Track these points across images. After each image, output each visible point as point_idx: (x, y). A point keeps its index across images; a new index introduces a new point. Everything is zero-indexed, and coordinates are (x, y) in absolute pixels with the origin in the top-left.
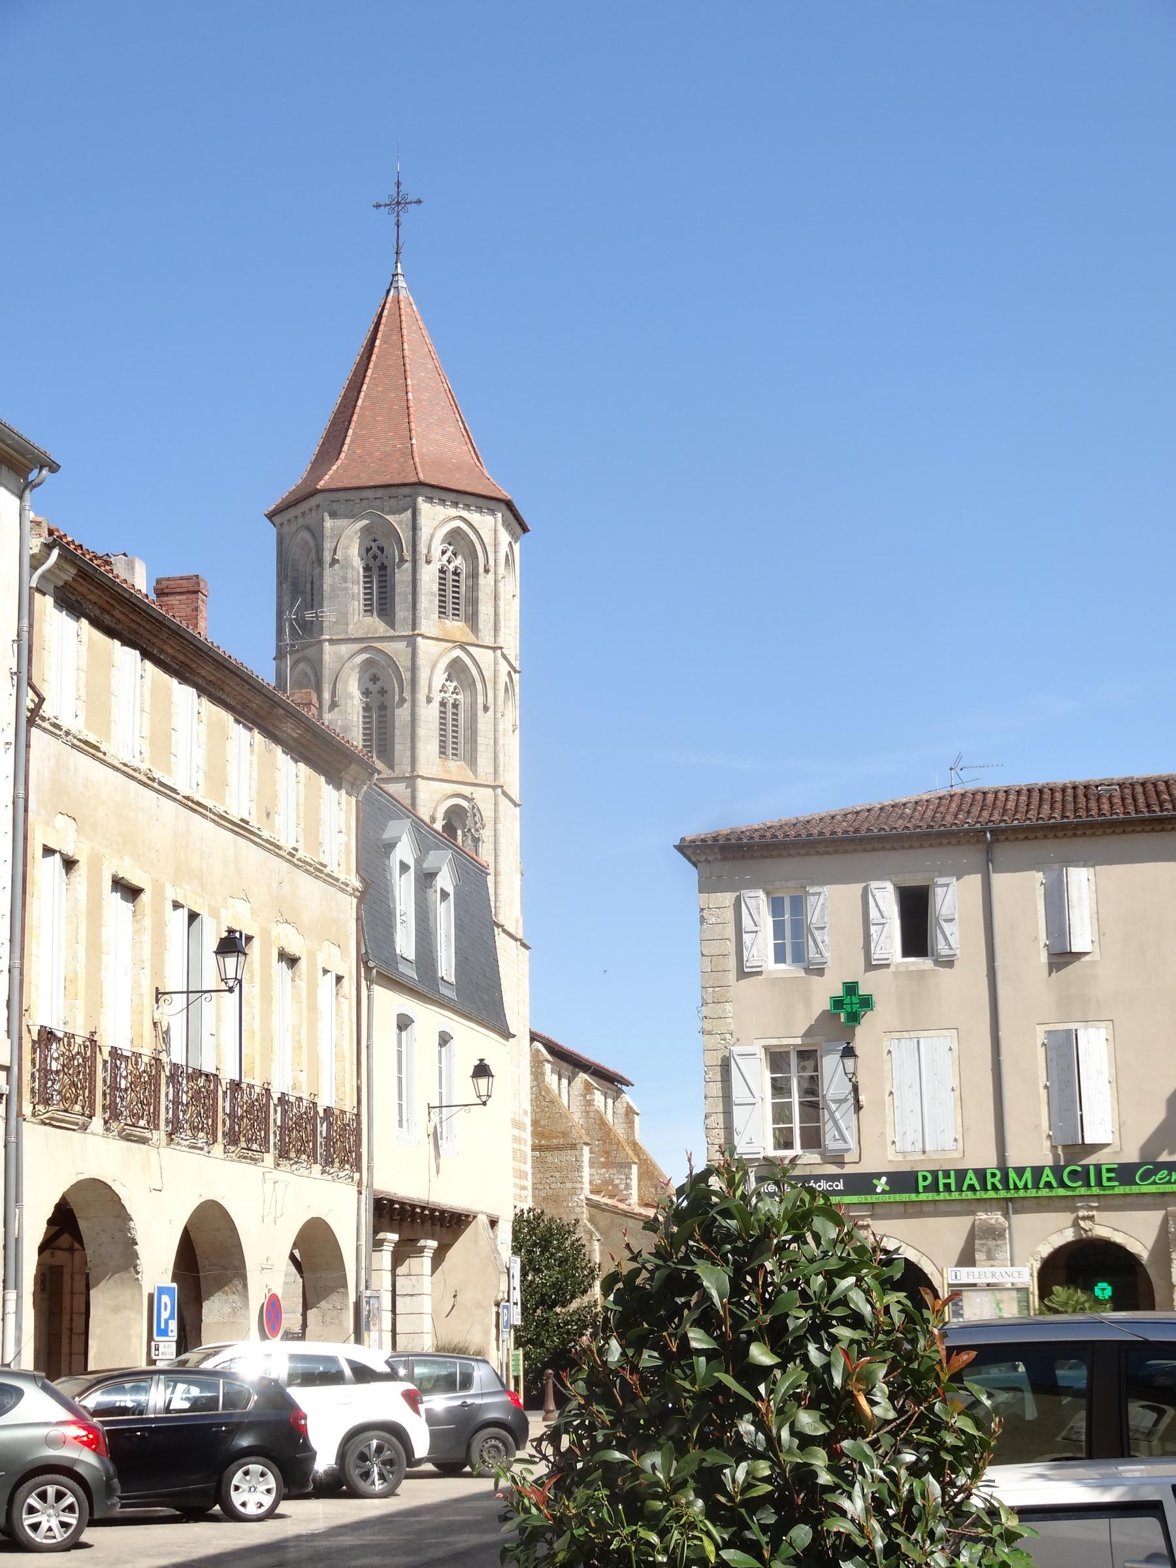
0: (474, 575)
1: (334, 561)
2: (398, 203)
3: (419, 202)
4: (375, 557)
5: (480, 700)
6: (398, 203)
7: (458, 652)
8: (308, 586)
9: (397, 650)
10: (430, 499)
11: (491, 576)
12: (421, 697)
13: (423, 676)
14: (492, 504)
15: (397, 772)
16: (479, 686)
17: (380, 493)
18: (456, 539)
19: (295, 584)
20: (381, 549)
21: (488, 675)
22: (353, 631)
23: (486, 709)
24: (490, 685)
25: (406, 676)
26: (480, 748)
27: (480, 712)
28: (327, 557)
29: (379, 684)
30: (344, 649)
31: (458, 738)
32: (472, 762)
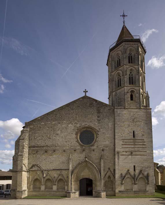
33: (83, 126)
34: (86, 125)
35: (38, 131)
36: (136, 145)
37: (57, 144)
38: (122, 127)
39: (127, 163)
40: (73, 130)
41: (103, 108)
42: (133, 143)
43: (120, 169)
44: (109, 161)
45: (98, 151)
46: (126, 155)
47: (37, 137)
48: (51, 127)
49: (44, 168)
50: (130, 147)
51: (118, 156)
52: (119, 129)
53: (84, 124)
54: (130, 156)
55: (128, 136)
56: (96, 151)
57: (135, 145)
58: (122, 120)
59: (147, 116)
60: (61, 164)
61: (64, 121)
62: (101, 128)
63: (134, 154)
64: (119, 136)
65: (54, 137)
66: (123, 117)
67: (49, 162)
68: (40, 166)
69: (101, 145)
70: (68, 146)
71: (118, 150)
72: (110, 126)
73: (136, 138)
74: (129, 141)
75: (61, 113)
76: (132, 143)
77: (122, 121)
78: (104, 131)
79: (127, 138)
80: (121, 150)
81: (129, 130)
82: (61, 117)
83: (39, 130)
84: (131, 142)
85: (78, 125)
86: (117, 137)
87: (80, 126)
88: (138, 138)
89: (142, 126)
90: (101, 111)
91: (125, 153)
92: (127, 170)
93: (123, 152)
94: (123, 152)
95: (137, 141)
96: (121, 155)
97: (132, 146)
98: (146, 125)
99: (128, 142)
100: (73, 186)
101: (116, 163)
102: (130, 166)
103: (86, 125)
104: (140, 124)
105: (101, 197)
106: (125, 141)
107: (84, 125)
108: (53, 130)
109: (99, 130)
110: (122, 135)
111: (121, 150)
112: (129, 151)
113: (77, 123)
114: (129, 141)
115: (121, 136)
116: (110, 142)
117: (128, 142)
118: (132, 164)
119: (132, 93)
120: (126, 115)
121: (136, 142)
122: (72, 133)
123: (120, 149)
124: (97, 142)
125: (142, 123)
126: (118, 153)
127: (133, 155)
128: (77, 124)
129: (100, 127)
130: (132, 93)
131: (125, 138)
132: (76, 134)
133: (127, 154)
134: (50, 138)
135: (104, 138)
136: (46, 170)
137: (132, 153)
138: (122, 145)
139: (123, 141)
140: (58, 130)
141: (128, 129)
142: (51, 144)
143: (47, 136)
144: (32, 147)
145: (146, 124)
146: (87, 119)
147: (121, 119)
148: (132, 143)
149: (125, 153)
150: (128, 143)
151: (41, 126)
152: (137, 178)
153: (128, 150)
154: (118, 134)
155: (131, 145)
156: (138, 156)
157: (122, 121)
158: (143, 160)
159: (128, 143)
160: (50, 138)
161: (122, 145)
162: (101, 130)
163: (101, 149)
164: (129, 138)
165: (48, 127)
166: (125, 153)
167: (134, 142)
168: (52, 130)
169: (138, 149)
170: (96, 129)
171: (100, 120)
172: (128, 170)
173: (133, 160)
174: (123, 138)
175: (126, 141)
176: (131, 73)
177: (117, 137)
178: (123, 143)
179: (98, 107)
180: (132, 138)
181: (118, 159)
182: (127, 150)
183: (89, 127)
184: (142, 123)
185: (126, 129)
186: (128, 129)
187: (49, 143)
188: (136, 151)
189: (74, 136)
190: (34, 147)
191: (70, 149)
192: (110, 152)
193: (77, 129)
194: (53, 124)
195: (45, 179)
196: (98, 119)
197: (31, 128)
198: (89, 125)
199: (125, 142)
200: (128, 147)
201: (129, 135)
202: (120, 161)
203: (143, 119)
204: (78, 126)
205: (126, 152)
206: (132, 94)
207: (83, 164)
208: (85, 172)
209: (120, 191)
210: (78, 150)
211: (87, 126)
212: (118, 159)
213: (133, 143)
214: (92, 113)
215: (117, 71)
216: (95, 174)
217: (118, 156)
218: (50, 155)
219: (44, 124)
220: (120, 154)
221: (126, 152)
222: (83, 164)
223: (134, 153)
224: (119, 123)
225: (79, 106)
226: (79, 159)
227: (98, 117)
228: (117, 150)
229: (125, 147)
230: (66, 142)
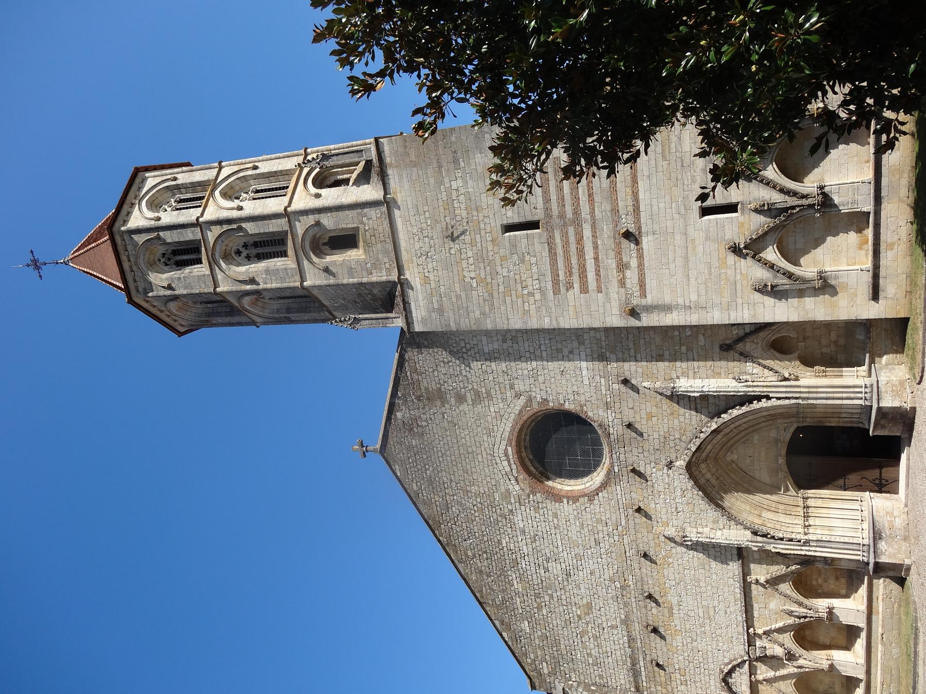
0: (178, 188)
1: (170, 287)
2: (36, 264)
3: (32, 252)
4: (169, 259)
5: (250, 172)
6: (36, 264)
7: (217, 193)
8: (209, 305)
9: (212, 235)
10: (125, 222)
11: (179, 176)
12: (235, 214)
13: (225, 214)
14: (138, 180)
15: (287, 228)
16: (241, 174)
17: (124, 258)
18: (154, 205)
19: (209, 315)
20: (164, 254)
21: (236, 168)
22: (208, 272)
23: (256, 168)
24: (242, 167)
25: (226, 227)
26: (280, 168)
27: (257, 171)
28: (168, 292)
29: (241, 250)
30: (220, 276)
31: (275, 184)
32: (287, 173)
33: (514, 467)
34: (506, 455)
35: (562, 646)
36: (577, 212)
37: (612, 580)
38: (495, 295)
39: (686, 258)
40: (537, 509)
41: (415, 376)
42: (571, 231)
43: (725, 300)
44: (684, 349)
45: (631, 406)
46: (641, 266)
47: (589, 655)
48: (537, 596)
49: (739, 650)
50: (596, 247)
51: (650, 309)
52: (503, 308)
53: (505, 463)
54: (646, 242)
55: (533, 260)
56: (629, 416)
57: (577, 221)
58: (458, 297)
59: (413, 158)
60: (714, 577)
61: (504, 544)
62: (512, 387)
63: (631, 219)
64: (538, 309)
65: (583, 590)
66: (442, 289)
67: (702, 625)
68: (726, 661)
69: (597, 389)
70: (616, 538)
71: (616, 311)
72: (496, 346)
73: (539, 215)
74: (560, 250)
75: (470, 553)
76: (572, 239)
77: (463, 295)
78: (526, 372)
79: (548, 267)
80: (614, 295)
81: (503, 258)
82: (486, 552)
83: (557, 643)
84: (566, 244)
85: (515, 488)
86: (547, 320)
87: (517, 480)
88: (540, 204)
89: (470, 183)
90: (434, 386)
91: (632, 276)
92: (731, 258)
93: (622, 283)
94: (622, 283)
95: (554, 205)
96: (643, 294)
97: (587, 233)
98: (462, 164)
99: (567, 259)
100: (838, 519)
101: (694, 319)
102: (707, 238)
103: (506, 455)
104: (462, 198)
105: (914, 409)
106: (562, 277)
107: (509, 462)
108: (550, 592)
109: (522, 401)
110: (531, 294)
111: (614, 295)
112: (619, 253)
113: (503, 491)
114: (560, 250)
115: (538, 296)
116: (575, 344)
117: (567, 259)
118: (691, 231)
119: (324, 244)
120: (432, 278)
121: (562, 216)
122: (555, 515)
123: (608, 299)
124: (581, 406)
125: (454, 185)
126: (633, 313)
127: (640, 228)
128: (508, 491)
129: (509, 394)
130: (324, 244)
131: (549, 278)
132: (557, 497)
133: (634, 263)
134: (589, 606)
135: (559, 377)
136: (751, 643)
137: (628, 235)
138: (584, 289)
139: (567, 290)
140: (547, 570)
141: (498, 262)
142: (613, 606)
143: (579, 617)
144: (636, 682)
145: (456, 161)
146: (479, 452)
147: (454, 299)
148: (572, 239)
149: (632, 276)
150: (574, 261)
151: (539, 633)
152: (782, 191)
153: (612, 254)
154: (532, 312)
155: (580, 240)
156: (641, 195)
157: (463, 295)
158: (664, 158)
159: (574, 261)
160: (589, 606)
161: (584, 289)
162: (522, 388)
163: (616, 386)
164: (546, 253)
165: (540, 608)
166: (628, 273)
167: (565, 225)
168: (551, 596)
169: (597, 198)
170: (521, 411)
171: (477, 394)
172: (735, 250)
173: (669, 224)
174: (549, 285)
175: (561, 273)
176: (238, 253)
177: (547, 320)
178: (576, 286)
179: (419, 400)
180: (544, 239)
181: (668, 308)
182: (612, 263)
183: (514, 443)
184: (454, 186)
185: (499, 269)
186: (498, 262)
187: (611, 613)
188: (615, 211)
189: (566, 508)
190: (636, 674)
191: (632, 532)
192: (631, 345)
193: (534, 494)
194: (524, 589)
195: (797, 650)
196: (470, 402)
197: (553, 673)
198: (504, 443)
199: (571, 275)
200: (596, 259)
201: (527, 258)
202: (681, 301)
203: (432, 181)
204: (517, 488)
205: (622, 267)
206: (326, 240)
207: (708, 476)
208: (748, 461)
209: (875, 295)
210: (634, 495)
211: (509, 449)
212: (668, 308)
213: (571, 231)
214: (446, 424)
215: (247, 310)
216: (764, 419)
217: (650, 309)
218: (671, 614)
219: (526, 623)
220: (635, 301)
221: (622, 267)
222: (708, 476)
223: (627, 223)
224: (477, 313)
225: (430, 482)
226: (679, 493)
227: (461, 399)
228: (615, 319)
229: (598, 274)
230: (598, 543)
